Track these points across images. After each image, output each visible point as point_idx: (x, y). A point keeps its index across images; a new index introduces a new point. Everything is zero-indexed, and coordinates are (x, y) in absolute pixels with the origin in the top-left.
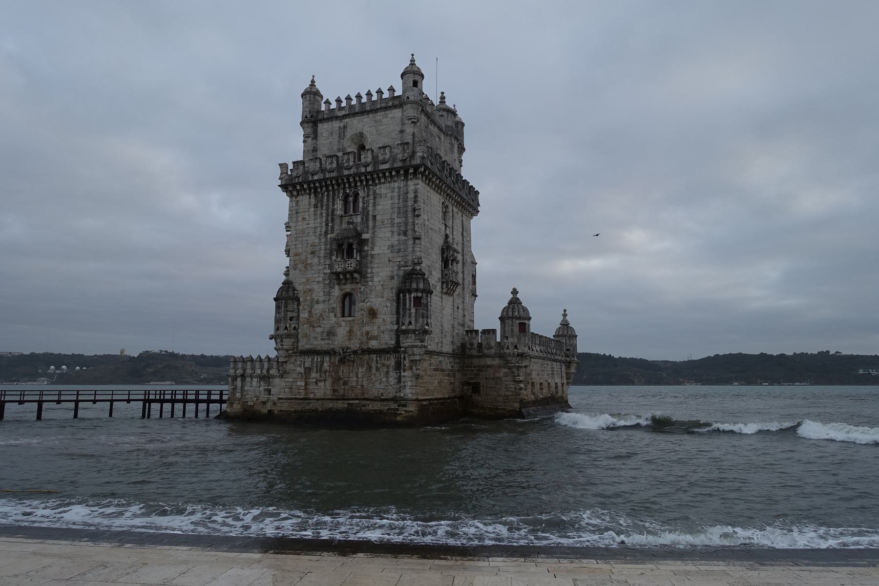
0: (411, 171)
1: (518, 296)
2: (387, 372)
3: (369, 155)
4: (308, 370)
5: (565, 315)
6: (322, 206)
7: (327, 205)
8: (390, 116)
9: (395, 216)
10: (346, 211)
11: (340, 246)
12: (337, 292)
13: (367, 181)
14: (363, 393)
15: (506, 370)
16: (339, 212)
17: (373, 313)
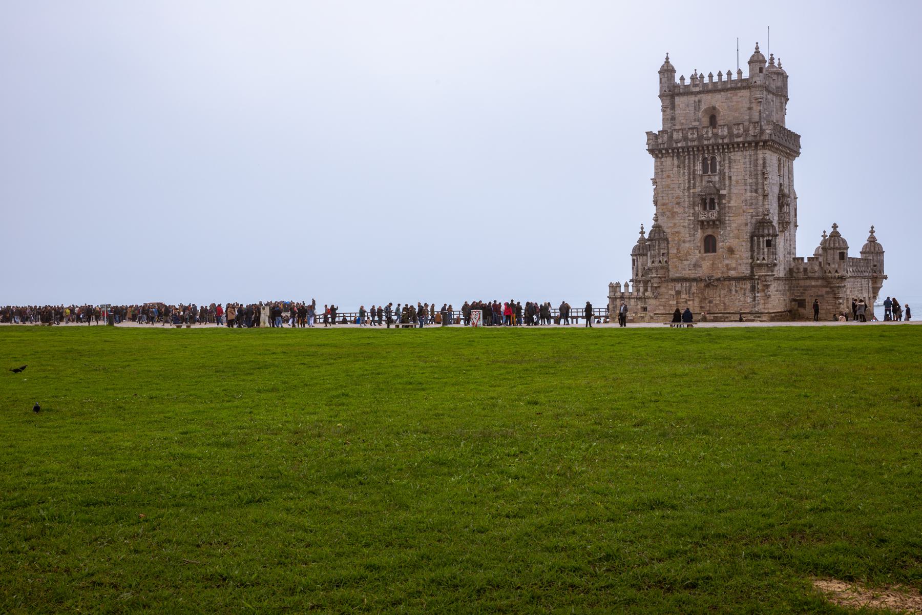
0: (761, 144)
1: (838, 229)
2: (745, 294)
3: (726, 130)
4: (678, 293)
5: (872, 232)
6: (684, 167)
7: (689, 166)
8: (740, 94)
9: (747, 177)
10: (705, 171)
11: (702, 199)
12: (699, 234)
13: (723, 149)
14: (725, 309)
15: (828, 289)
16: (699, 172)
17: (731, 251)
